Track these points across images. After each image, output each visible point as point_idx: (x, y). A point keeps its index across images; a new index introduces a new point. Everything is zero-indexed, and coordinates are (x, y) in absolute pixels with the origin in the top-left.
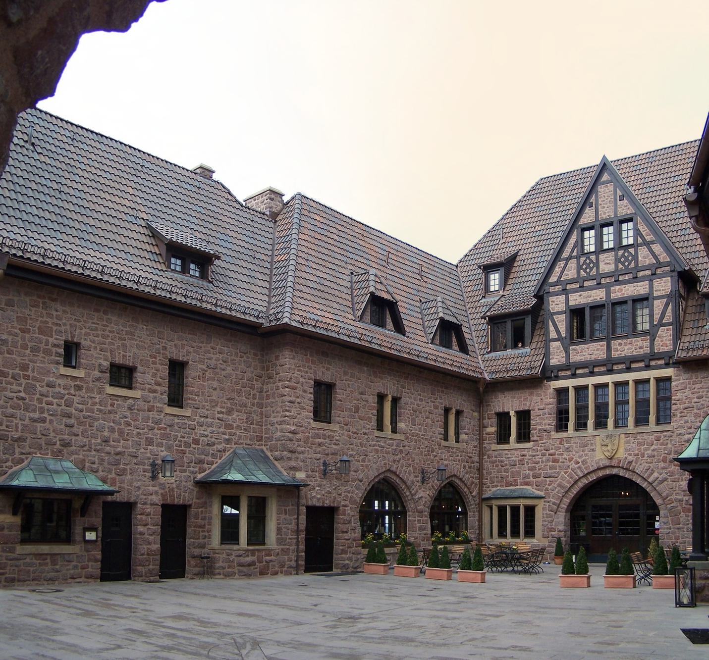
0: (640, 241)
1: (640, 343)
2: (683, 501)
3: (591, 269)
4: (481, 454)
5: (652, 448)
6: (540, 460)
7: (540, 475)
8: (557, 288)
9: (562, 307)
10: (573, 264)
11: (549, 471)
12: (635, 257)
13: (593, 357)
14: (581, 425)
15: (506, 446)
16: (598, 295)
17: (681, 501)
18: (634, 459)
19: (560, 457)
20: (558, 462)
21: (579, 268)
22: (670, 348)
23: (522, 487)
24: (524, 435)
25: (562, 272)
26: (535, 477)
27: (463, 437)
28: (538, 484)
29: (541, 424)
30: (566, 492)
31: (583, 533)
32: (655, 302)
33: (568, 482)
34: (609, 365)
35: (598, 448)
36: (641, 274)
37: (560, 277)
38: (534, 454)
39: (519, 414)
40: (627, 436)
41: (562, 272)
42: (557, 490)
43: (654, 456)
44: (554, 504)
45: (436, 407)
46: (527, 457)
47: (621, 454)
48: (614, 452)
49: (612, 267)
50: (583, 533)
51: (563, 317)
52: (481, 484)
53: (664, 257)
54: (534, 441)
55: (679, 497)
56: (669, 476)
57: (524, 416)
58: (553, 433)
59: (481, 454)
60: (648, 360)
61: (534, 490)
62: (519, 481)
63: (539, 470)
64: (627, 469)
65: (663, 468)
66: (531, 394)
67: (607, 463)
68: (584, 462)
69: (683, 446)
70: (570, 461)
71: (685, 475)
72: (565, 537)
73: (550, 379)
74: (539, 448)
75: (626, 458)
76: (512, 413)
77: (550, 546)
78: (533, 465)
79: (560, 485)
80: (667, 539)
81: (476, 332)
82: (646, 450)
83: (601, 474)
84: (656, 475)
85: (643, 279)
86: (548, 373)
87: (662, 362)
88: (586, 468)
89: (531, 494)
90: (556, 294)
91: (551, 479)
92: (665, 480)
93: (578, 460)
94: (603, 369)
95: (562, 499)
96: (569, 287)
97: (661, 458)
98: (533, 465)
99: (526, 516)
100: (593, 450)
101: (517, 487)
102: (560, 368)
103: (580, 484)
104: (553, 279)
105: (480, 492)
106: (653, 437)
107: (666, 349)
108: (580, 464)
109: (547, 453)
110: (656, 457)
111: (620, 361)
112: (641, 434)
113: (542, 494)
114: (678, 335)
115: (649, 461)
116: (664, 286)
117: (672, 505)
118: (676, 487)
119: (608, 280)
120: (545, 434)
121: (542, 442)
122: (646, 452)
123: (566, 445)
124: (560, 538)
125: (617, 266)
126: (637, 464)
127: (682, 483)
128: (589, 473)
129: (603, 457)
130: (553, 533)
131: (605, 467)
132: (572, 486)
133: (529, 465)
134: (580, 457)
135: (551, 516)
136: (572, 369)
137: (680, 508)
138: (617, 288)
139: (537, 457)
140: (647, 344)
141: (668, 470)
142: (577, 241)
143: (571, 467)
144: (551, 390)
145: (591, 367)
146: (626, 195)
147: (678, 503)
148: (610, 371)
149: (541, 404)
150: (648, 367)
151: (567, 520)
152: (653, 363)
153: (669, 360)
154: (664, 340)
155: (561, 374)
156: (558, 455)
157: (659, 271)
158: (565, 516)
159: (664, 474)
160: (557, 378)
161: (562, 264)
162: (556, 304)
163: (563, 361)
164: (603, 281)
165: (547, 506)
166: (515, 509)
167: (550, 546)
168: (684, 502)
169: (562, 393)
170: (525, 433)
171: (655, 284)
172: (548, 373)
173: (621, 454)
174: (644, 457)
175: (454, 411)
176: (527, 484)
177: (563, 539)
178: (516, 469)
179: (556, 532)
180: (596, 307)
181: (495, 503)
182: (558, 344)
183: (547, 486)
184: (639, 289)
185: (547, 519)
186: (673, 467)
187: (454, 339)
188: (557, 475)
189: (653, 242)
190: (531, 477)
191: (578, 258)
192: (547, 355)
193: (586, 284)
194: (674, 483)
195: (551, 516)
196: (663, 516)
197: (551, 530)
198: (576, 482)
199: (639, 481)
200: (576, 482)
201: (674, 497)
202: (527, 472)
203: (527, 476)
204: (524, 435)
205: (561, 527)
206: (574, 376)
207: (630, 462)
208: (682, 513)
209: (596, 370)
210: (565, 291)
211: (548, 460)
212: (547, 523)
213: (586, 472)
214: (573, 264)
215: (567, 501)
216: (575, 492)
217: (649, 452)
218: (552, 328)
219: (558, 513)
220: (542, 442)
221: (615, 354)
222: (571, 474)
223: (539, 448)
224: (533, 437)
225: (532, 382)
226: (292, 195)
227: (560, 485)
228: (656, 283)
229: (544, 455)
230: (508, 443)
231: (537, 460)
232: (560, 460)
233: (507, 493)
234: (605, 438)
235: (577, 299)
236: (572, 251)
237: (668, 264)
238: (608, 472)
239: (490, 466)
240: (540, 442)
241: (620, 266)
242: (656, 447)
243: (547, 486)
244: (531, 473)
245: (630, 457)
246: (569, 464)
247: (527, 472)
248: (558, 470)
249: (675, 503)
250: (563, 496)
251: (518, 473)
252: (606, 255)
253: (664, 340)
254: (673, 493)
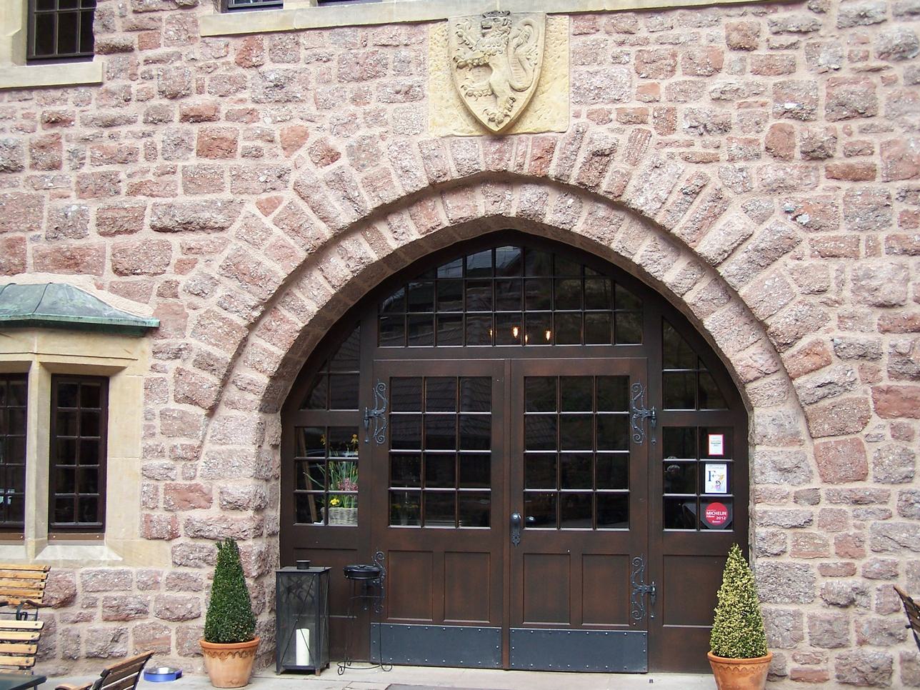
2: (876, 357)
5: (719, 82)
6: (140, 144)
7: (139, 218)
11: (182, 199)
17: (866, 355)
18: (623, 140)
19: (237, 125)
20: (229, 153)
23: (43, 278)
26: (110, 227)
28: (125, 264)
30: (270, 305)
31: (342, 517)
33: (281, 251)
35: (437, 86)
38: (113, 113)
40: (583, 24)
42: (220, 292)
43: (724, 128)
44: (205, 363)
46: (77, 130)
47: (555, 114)
48: (522, 99)
50: (342, 517)
54: (112, 50)
55: (862, 338)
56: (807, 227)
61: (105, 295)
62: (30, 247)
63: (135, 191)
64: (584, 192)
65: (776, 188)
67: (483, 157)
68: (363, 153)
69: (875, 78)
70: (291, 145)
71: (887, 223)
72: (258, 536)
74: (135, 87)
75: (580, 134)
77: (176, 583)
78: (104, 168)
80: (797, 553)
82: (685, 93)
84: (735, 220)
88: (370, 184)
89: (90, 312)
91: (191, 238)
92: (786, 246)
93: (333, 142)
95: (245, 341)
97: (762, 138)
98: (104, 168)
99: (59, 422)
100: (409, 94)
101: (19, 279)
103: (340, 268)
106: (719, 31)
108: (344, 161)
109: (176, 109)
110: (735, 132)
112: (658, 18)
113: (142, 312)
115: (698, 148)
117: (824, 376)
118: (842, 283)
120: (165, 15)
121: (150, 53)
122: (682, 109)
123: (273, 70)
124: (232, 543)
126: (635, 163)
127: (872, 264)
128: (384, 212)
129: (461, 125)
130: (197, 515)
132: (295, 277)
133: (87, 169)
134: (348, 124)
135: (187, 427)
137: (862, 391)
139: (123, 130)
141: (799, 196)
143: (293, 177)
147: (855, 365)
151: (266, 447)
156: (228, 118)
158: (262, 428)
159: (778, 216)
165: (170, 377)
167: (176, 583)
168: (885, 361)
170: (68, 20)
173: (555, 114)
174: (672, 129)
176: (72, 263)
177: (250, 548)
179: (214, 512)
183: (170, 275)
185: (166, 443)
186: (825, 183)
188: (220, 219)
190: (92, 229)
194: (833, 265)
195: (187, 427)
196: (771, 431)
197: (189, 497)
198: (317, 255)
199: (641, 251)
200: (317, 255)
201: (829, 335)
202: (74, 203)
203: (66, 227)
205: (243, 486)
208: (875, 420)
212: (167, 462)
213: (370, 204)
215: (270, 350)
216: (313, 308)
217: (703, 106)
219: (223, 411)
220: (150, 53)
222: (292, 211)
223: (135, 87)
224: (106, 27)
227: (234, 270)
229: (158, 119)
231: (127, 143)
232: (242, 144)
234: (477, 31)
238: (480, 205)
240: (140, 56)
242: (735, 81)
243: (170, 275)
244: (93, 208)
245: (603, 129)
246: (284, 161)
247: (74, 203)
248: (227, 195)
249: (837, 365)
250: (252, 326)
254: (825, 318)
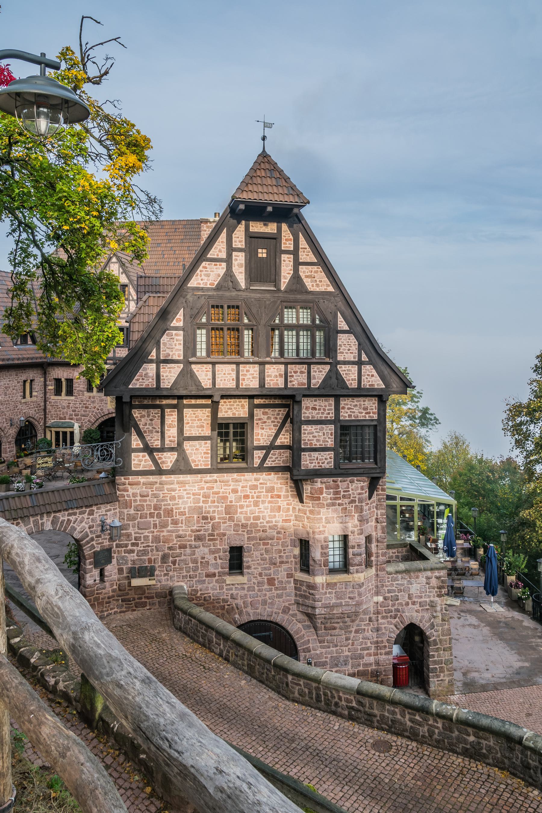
4: (45, 401)
15: (59, 397)
24: (70, 392)
26: (75, 415)
27: (34, 394)
45: (18, 382)
52: (45, 418)
57: (70, 381)
59: (45, 401)
66: (74, 370)
68: (102, 410)
76: (63, 380)
79: (89, 421)
105: (45, 423)
166: (65, 433)
175: (29, 381)
176: (71, 419)
178: (65, 410)
181: (53, 430)
198: (97, 420)
200: (97, 420)
203: (71, 415)
204: (70, 392)
211: (83, 407)
227: (89, 421)
229: (80, 404)
230: (61, 395)
233: (60, 424)
239: (50, 407)
251: (67, 413)
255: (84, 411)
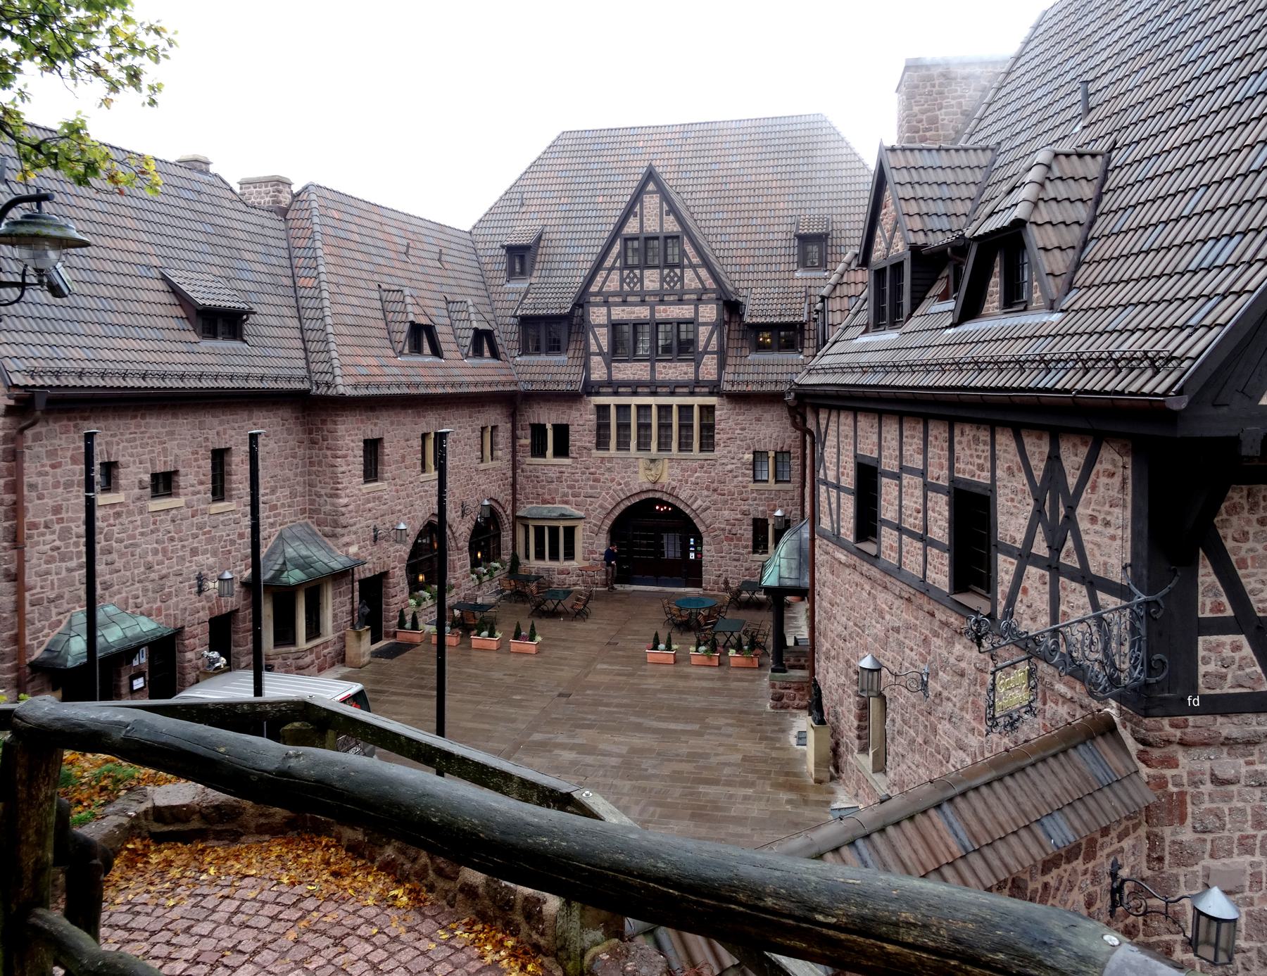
0: (686, 262)
1: (684, 369)
3: (635, 284)
4: (514, 468)
8: (598, 299)
9: (603, 320)
10: (615, 275)
12: (681, 278)
13: (637, 377)
14: (623, 445)
16: (642, 313)
21: (622, 281)
22: (714, 377)
25: (604, 283)
29: (580, 440)
32: (701, 328)
34: (653, 388)
35: (641, 470)
36: (686, 297)
37: (602, 288)
39: (555, 427)
41: (604, 283)
49: (657, 286)
51: (605, 330)
52: (515, 500)
53: (710, 283)
58: (594, 451)
60: (693, 387)
66: (570, 408)
67: (650, 486)
68: (627, 484)
73: (590, 394)
76: (549, 427)
79: (601, 506)
81: (507, 337)
82: (690, 476)
83: (644, 497)
85: (688, 302)
86: (590, 389)
87: (706, 390)
90: (597, 304)
94: (646, 390)
96: (611, 299)
102: (601, 384)
103: (623, 507)
104: (594, 289)
107: (711, 378)
111: (664, 384)
113: (582, 514)
114: (722, 365)
116: (709, 312)
119: (652, 298)
125: (662, 286)
131: (648, 491)
134: (623, 478)
136: (615, 387)
138: (662, 308)
140: (691, 370)
142: (619, 253)
144: (592, 406)
145: (634, 388)
146: (673, 210)
148: (654, 394)
149: (581, 421)
150: (692, 394)
152: (697, 390)
153: (714, 389)
154: (709, 368)
155: (604, 390)
157: (704, 297)
160: (598, 394)
161: (604, 273)
162: (598, 315)
163: (605, 377)
164: (647, 298)
169: (603, 410)
171: (701, 309)
172: (590, 389)
173: (665, 479)
176: (566, 503)
180: (636, 325)
182: (599, 358)
184: (686, 312)
187: (485, 345)
189: (699, 266)
191: (621, 269)
192: (586, 366)
193: (629, 299)
197: (592, 552)
198: (618, 504)
200: (618, 504)
203: (565, 495)
206: (616, 394)
207: (674, 488)
209: (639, 390)
210: (606, 303)
214: (615, 275)
215: (609, 522)
218: (592, 341)
221: (659, 377)
225: (571, 398)
226: (303, 184)
228: (702, 308)
229: (583, 473)
230: (544, 456)
235: (619, 313)
236: (615, 262)
237: (714, 291)
239: (524, 481)
241: (666, 286)
251: (556, 490)
252: (651, 271)
253: (709, 368)
255: (592, 487)
